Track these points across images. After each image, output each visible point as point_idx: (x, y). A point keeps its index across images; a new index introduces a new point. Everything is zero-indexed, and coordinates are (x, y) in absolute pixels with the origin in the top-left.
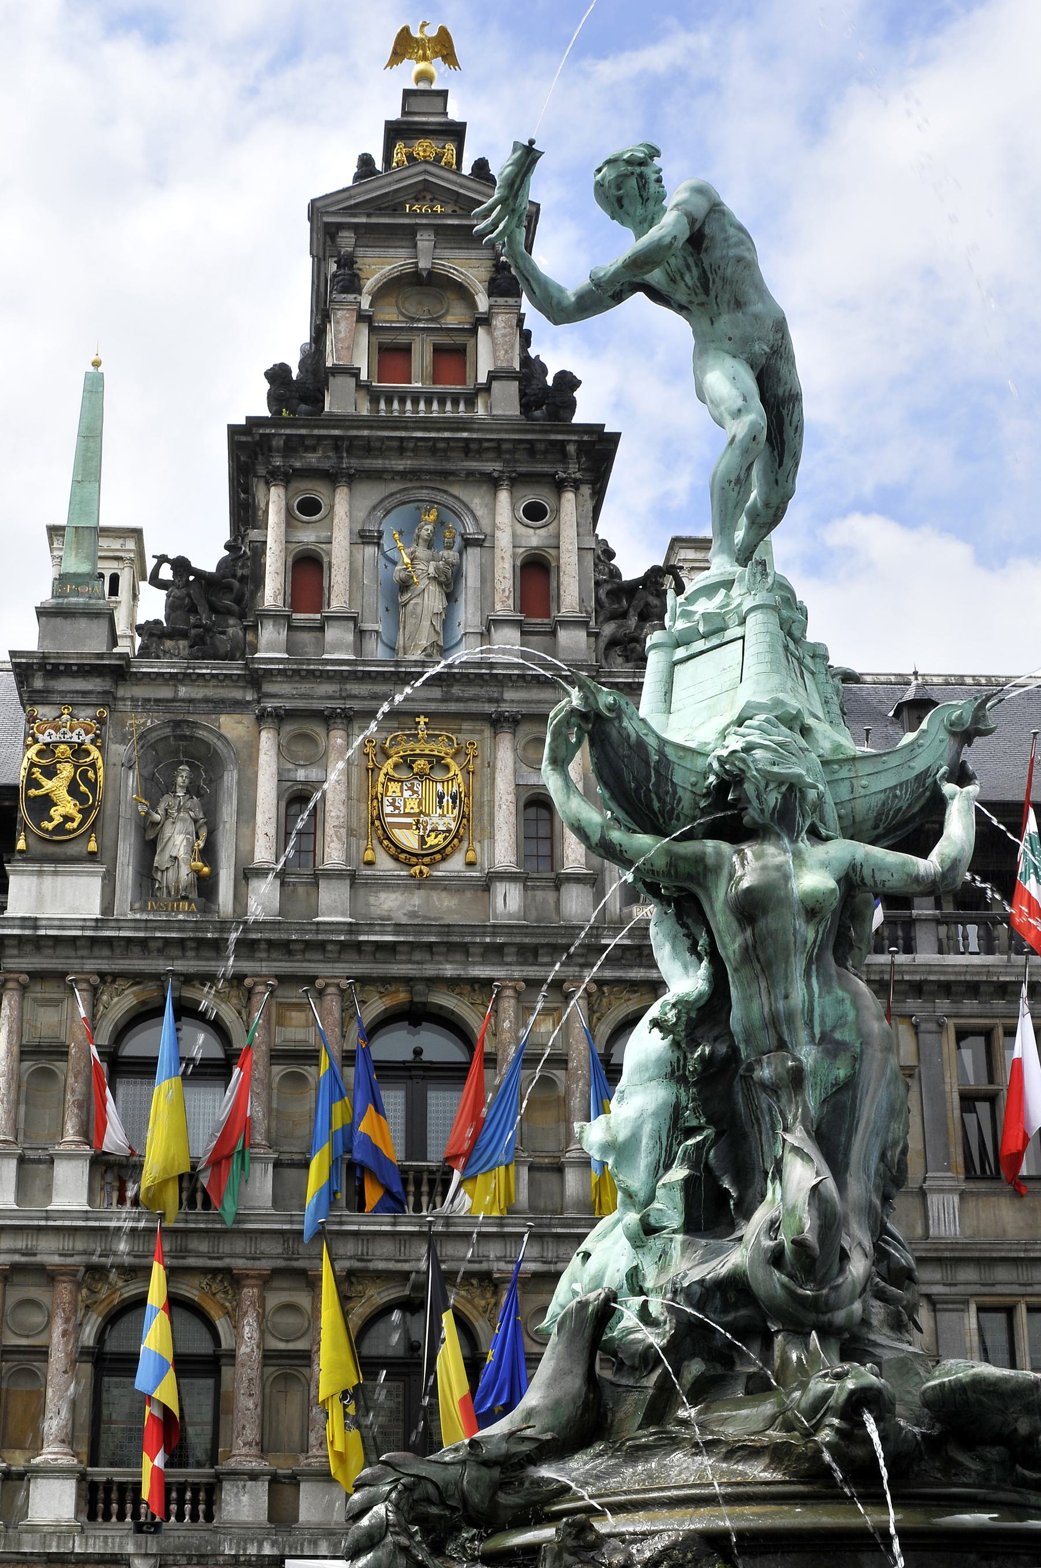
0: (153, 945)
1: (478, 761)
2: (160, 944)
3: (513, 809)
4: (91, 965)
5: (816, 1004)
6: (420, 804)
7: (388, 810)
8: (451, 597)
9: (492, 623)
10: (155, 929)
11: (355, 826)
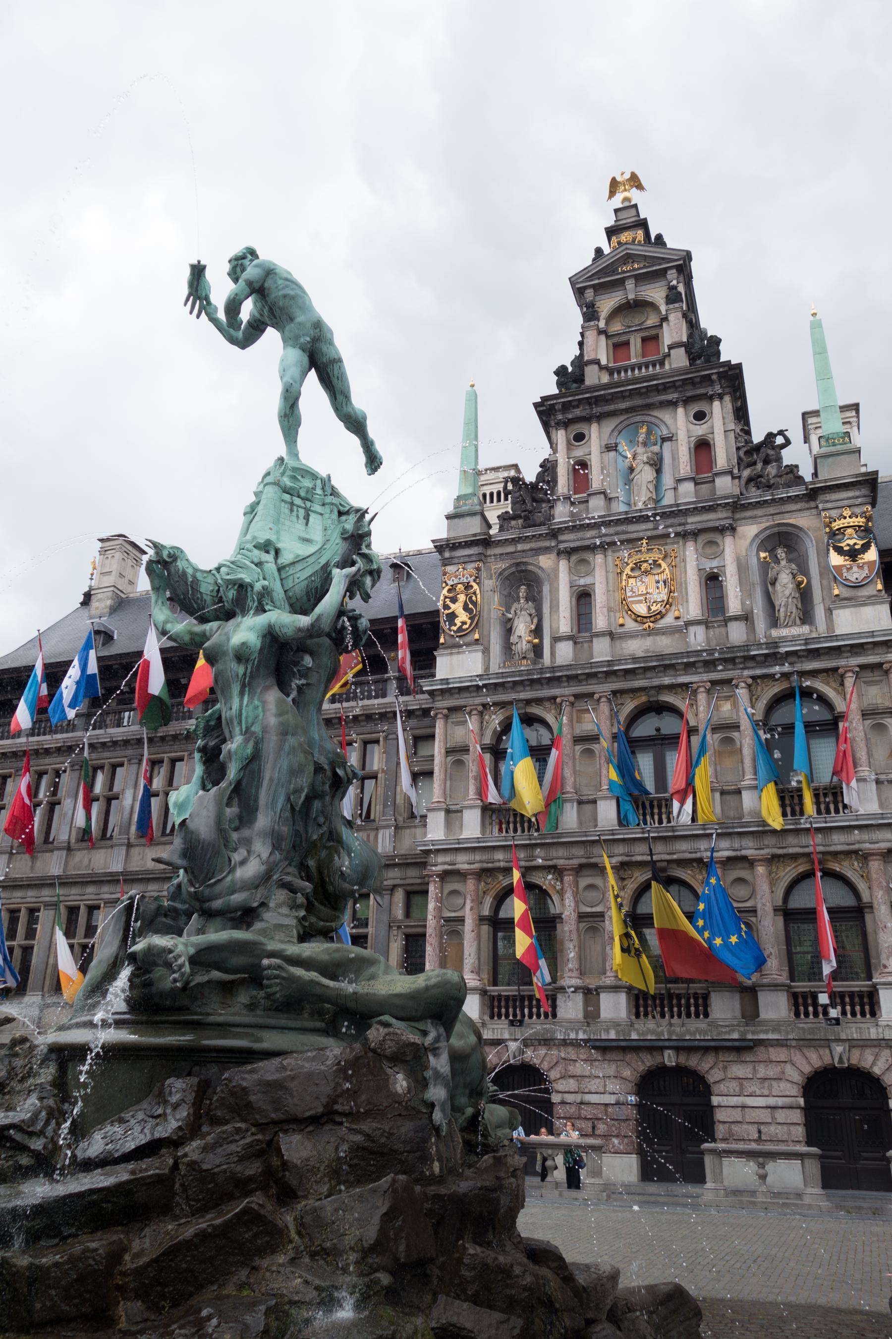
1: (678, 559)
2: (511, 684)
3: (697, 583)
4: (478, 700)
5: (243, 711)
6: (646, 588)
7: (629, 594)
8: (659, 471)
9: (679, 481)
10: (507, 677)
11: (612, 605)
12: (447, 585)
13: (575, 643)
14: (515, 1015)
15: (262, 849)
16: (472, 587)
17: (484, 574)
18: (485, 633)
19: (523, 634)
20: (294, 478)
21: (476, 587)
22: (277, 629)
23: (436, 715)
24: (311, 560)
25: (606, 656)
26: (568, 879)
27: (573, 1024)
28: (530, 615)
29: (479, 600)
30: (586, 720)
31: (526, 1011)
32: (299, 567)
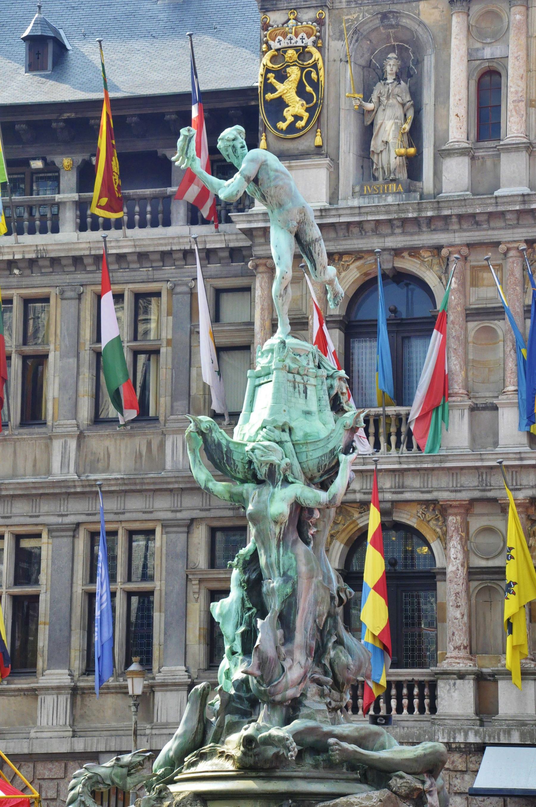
0: (368, 227)
5: (281, 560)
12: (269, 48)
13: (473, 158)
14: (377, 709)
15: (300, 656)
16: (311, 55)
17: (328, 30)
18: (332, 134)
19: (391, 140)
20: (294, 360)
21: (317, 55)
22: (302, 500)
23: (256, 267)
24: (321, 444)
25: (520, 184)
26: (452, 520)
27: (460, 723)
28: (403, 105)
29: (322, 79)
30: (485, 282)
31: (393, 703)
32: (311, 447)
